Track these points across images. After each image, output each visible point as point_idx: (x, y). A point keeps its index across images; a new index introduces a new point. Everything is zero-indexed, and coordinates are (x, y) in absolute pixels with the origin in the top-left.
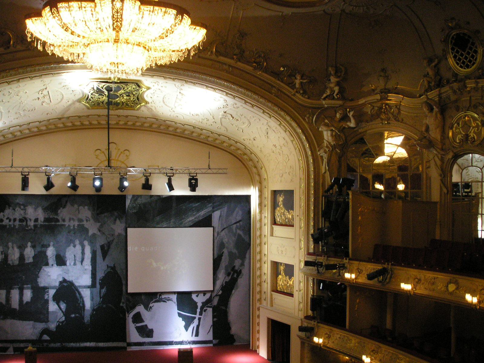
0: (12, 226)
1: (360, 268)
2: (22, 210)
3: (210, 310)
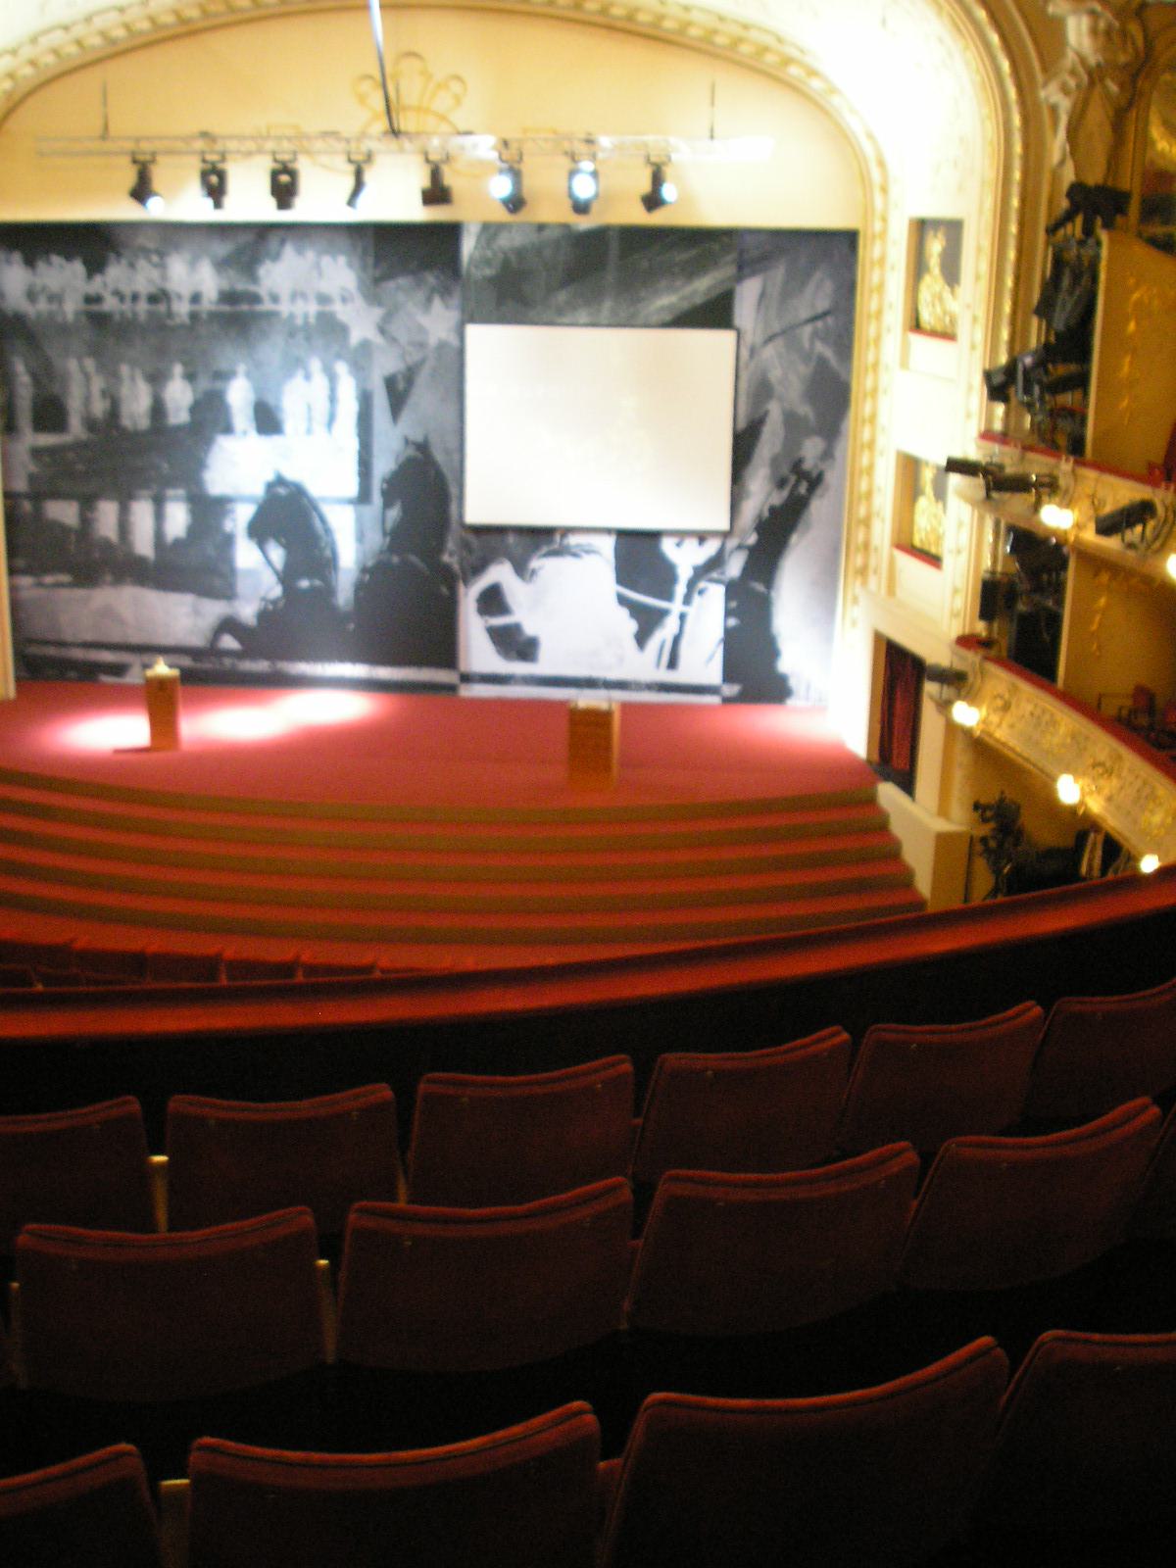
1: (1100, 493)
2: (156, 266)
3: (714, 597)
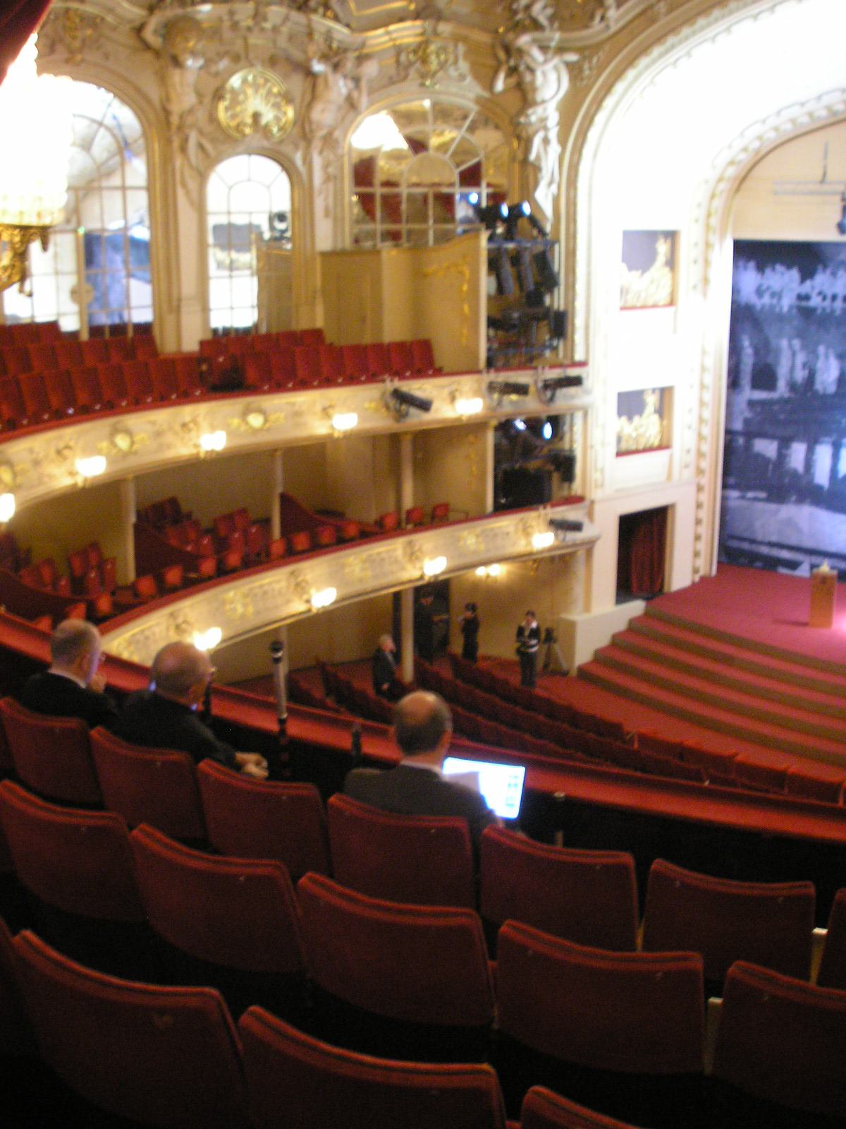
0: (828, 310)
